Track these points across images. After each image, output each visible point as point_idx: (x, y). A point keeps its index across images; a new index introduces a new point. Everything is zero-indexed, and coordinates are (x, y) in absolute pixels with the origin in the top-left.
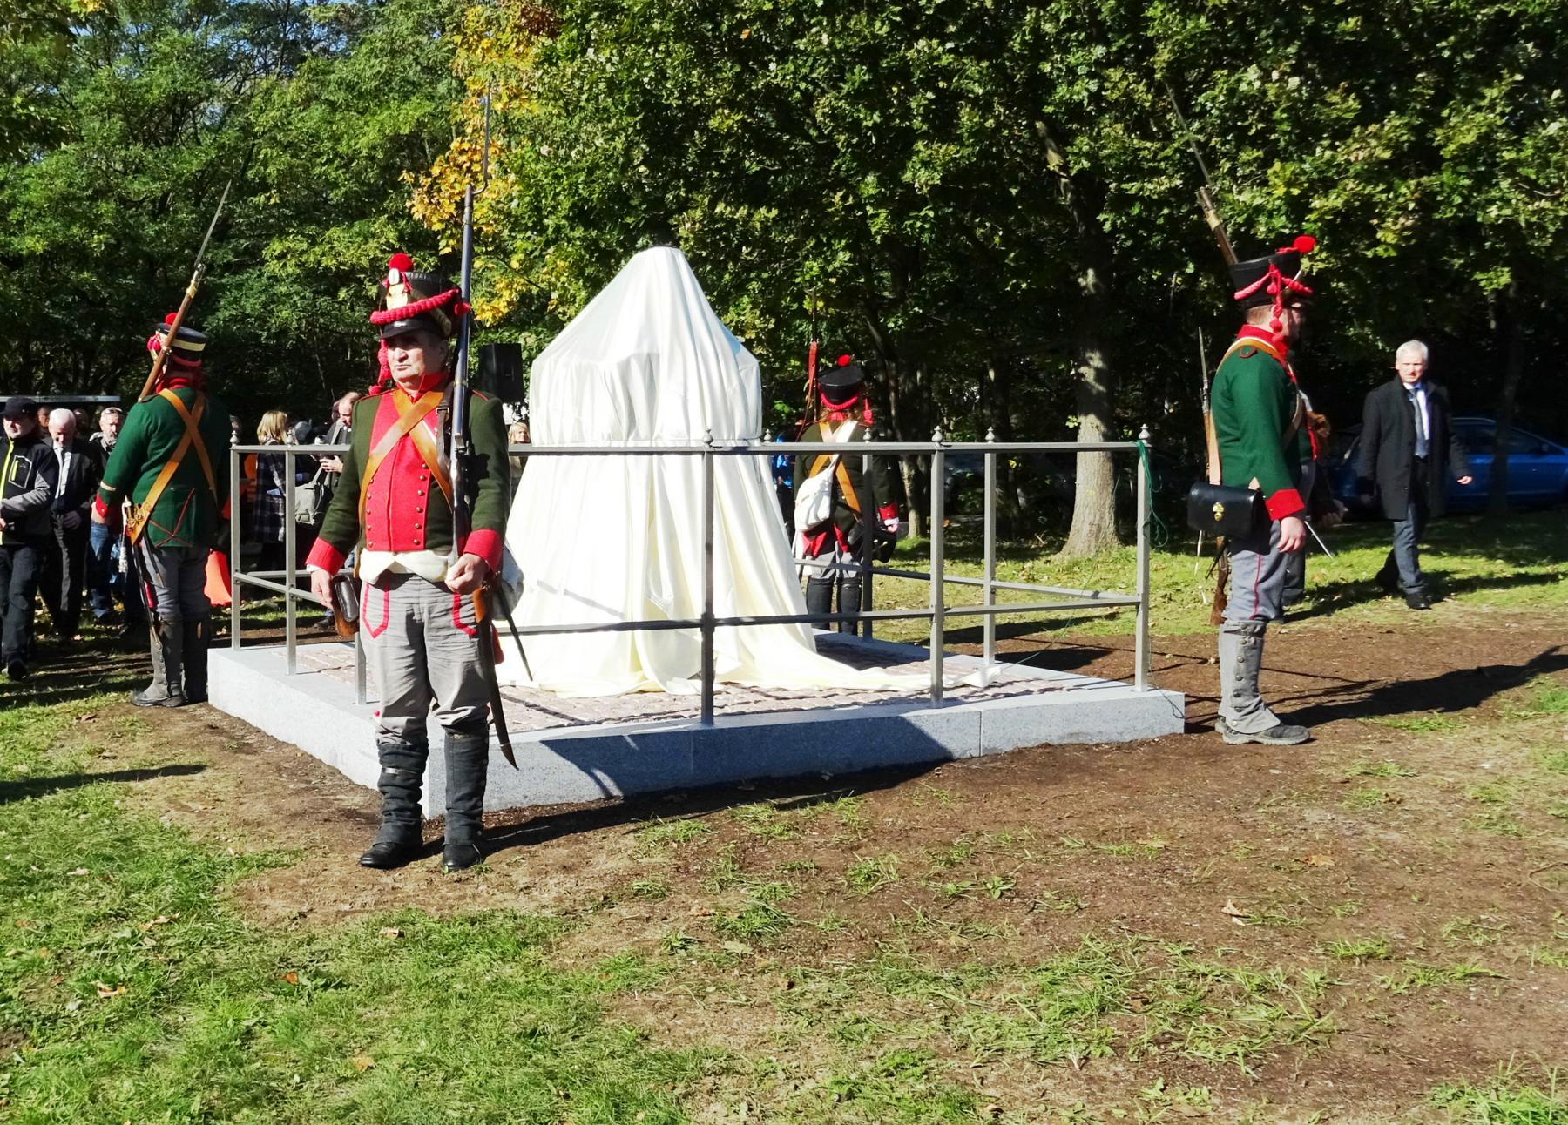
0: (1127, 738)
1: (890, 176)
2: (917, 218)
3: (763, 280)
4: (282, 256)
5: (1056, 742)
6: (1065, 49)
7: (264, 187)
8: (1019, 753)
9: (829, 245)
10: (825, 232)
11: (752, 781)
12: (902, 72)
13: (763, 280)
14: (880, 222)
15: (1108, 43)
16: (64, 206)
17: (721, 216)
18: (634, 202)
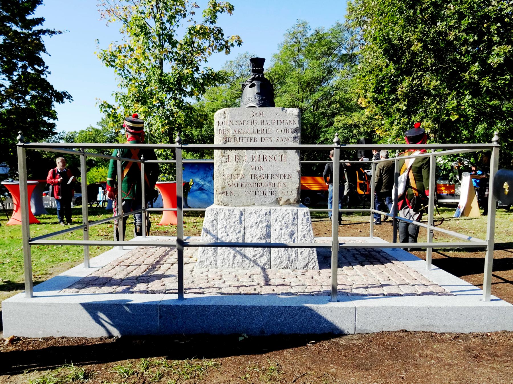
0: (466, 331)
1: (483, 63)
2: (503, 79)
3: (437, 109)
5: (410, 329)
7: (335, 102)
9: (463, 94)
14: (485, 82)
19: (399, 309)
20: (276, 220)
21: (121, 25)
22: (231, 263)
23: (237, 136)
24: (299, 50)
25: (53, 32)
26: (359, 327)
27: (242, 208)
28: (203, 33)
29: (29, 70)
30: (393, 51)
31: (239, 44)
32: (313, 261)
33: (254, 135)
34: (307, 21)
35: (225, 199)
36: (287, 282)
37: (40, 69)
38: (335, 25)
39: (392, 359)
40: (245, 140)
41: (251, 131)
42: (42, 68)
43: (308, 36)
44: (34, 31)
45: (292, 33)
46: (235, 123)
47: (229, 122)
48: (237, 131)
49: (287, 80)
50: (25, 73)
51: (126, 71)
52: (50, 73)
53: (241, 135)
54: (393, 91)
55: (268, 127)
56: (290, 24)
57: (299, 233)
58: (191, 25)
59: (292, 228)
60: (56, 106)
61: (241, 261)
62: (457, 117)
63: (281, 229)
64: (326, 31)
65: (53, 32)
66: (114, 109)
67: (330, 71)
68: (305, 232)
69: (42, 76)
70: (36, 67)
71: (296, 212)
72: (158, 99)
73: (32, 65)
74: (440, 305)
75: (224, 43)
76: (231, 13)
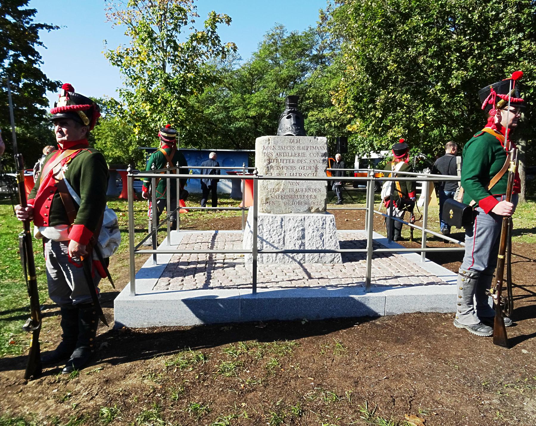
1: (445, 84)
2: (458, 97)
3: (407, 118)
4: (312, 116)
6: (508, 35)
7: (309, 98)
8: (404, 316)
9: (428, 106)
10: (427, 102)
11: (265, 322)
12: (448, 47)
13: (407, 118)
14: (445, 98)
15: (523, 31)
16: (260, 105)
17: (391, 98)
18: (365, 94)
19: (416, 297)
20: (309, 225)
21: (127, 29)
22: (274, 259)
23: (279, 158)
24: (277, 50)
25: (50, 27)
26: (388, 311)
27: (282, 215)
28: (203, 40)
29: (21, 59)
30: (373, 69)
31: (235, 51)
32: (338, 257)
33: (292, 158)
34: (284, 25)
35: (269, 208)
36: (324, 275)
37: (33, 59)
38: (308, 29)
39: (418, 335)
40: (285, 161)
41: (290, 154)
42: (35, 58)
43: (285, 38)
44: (32, 25)
45: (270, 34)
46: (277, 148)
47: (272, 147)
48: (279, 154)
49: (266, 77)
50: (16, 61)
51: (131, 71)
52: (43, 63)
53: (282, 158)
54: (373, 101)
55: (303, 151)
56: (269, 27)
57: (327, 235)
58: (193, 32)
59: (321, 231)
60: (48, 94)
61: (282, 257)
62: (423, 125)
63: (313, 232)
64: (300, 34)
65: (50, 27)
66: (121, 106)
67: (304, 69)
68: (331, 234)
69: (34, 65)
70: (30, 57)
71: (324, 218)
72: (163, 97)
73: (25, 55)
74: (444, 293)
75: (221, 49)
76: (229, 24)
